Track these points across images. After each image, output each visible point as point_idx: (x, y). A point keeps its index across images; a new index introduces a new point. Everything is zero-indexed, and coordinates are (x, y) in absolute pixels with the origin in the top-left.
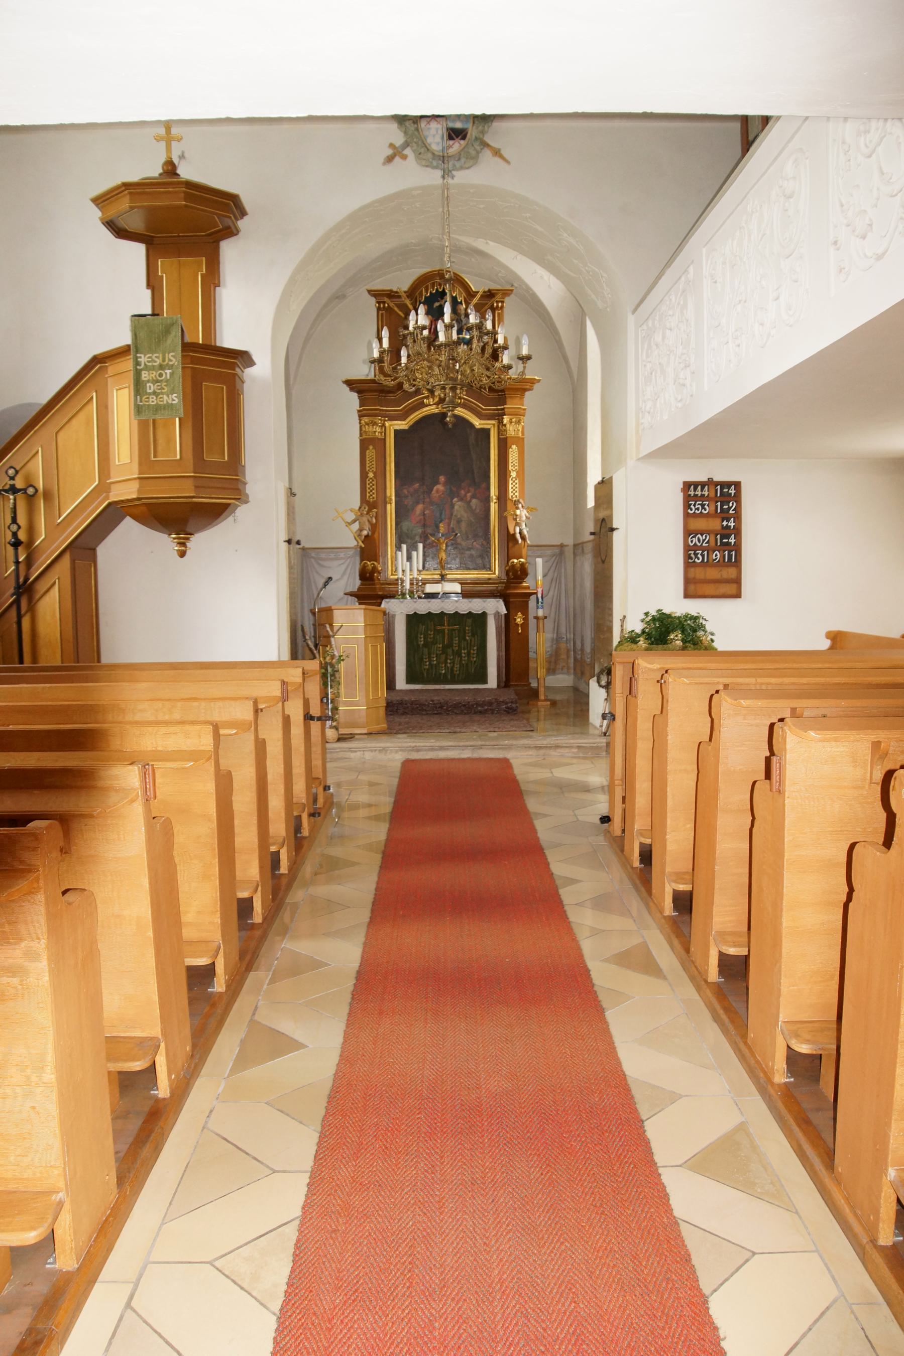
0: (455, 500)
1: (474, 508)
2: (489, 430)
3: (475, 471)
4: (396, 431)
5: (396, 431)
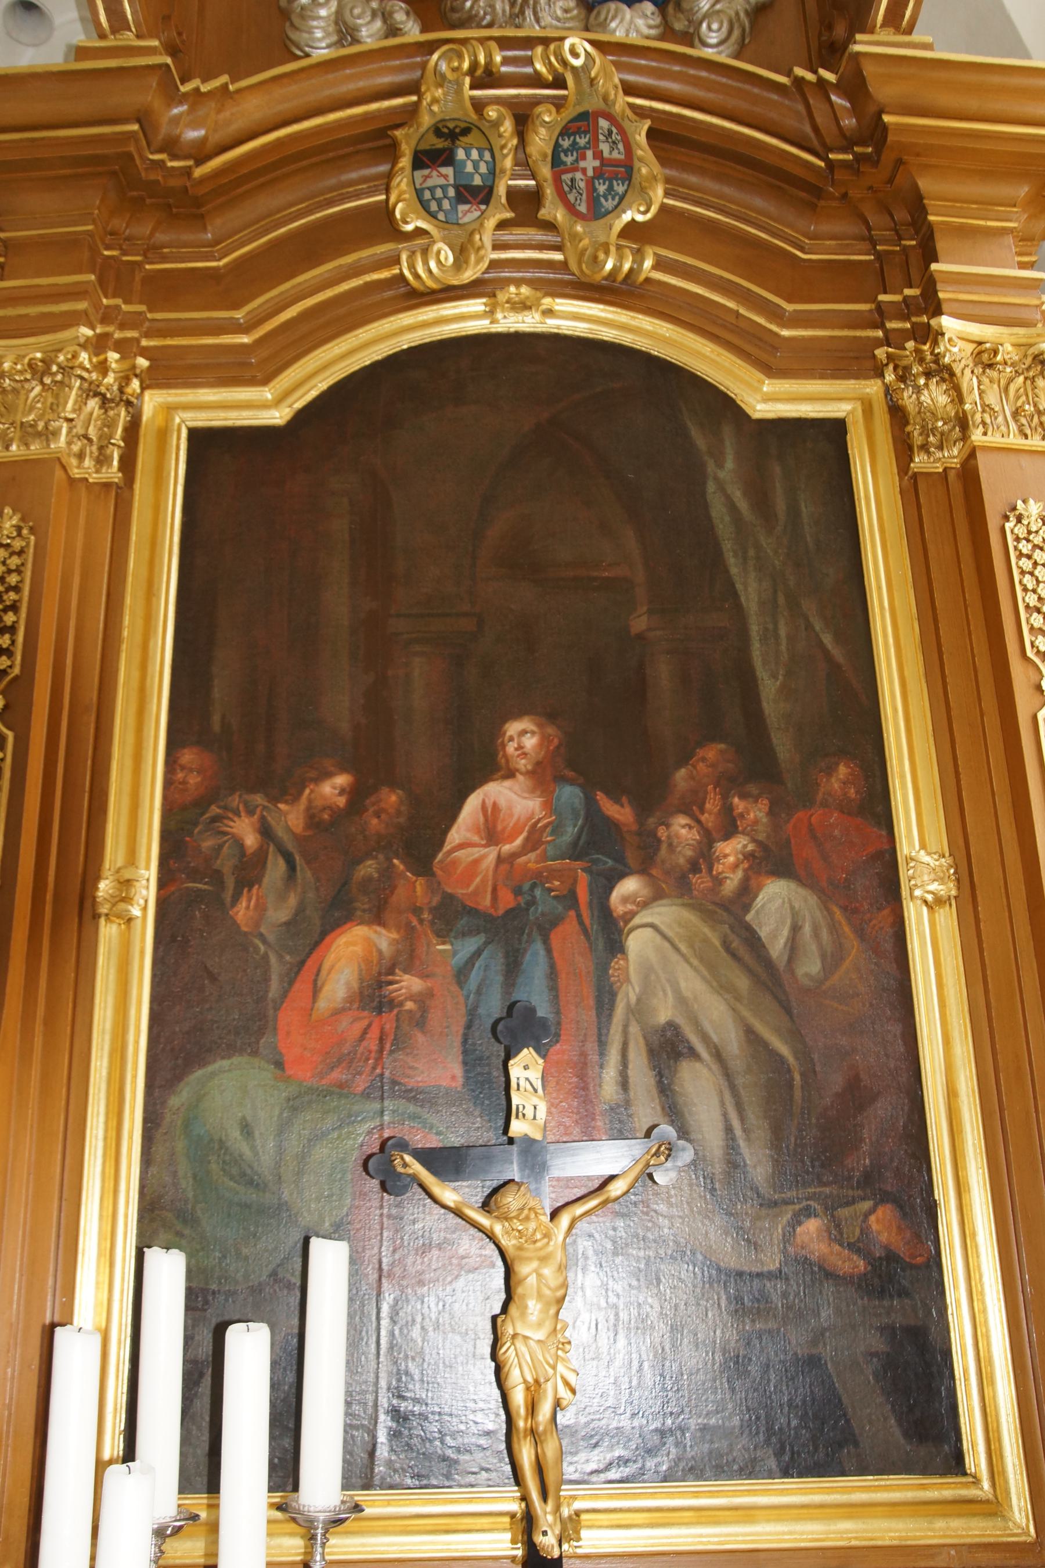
0: (630, 886)
1: (777, 948)
2: (836, 429)
3: (769, 687)
4: (199, 438)
5: (199, 438)
